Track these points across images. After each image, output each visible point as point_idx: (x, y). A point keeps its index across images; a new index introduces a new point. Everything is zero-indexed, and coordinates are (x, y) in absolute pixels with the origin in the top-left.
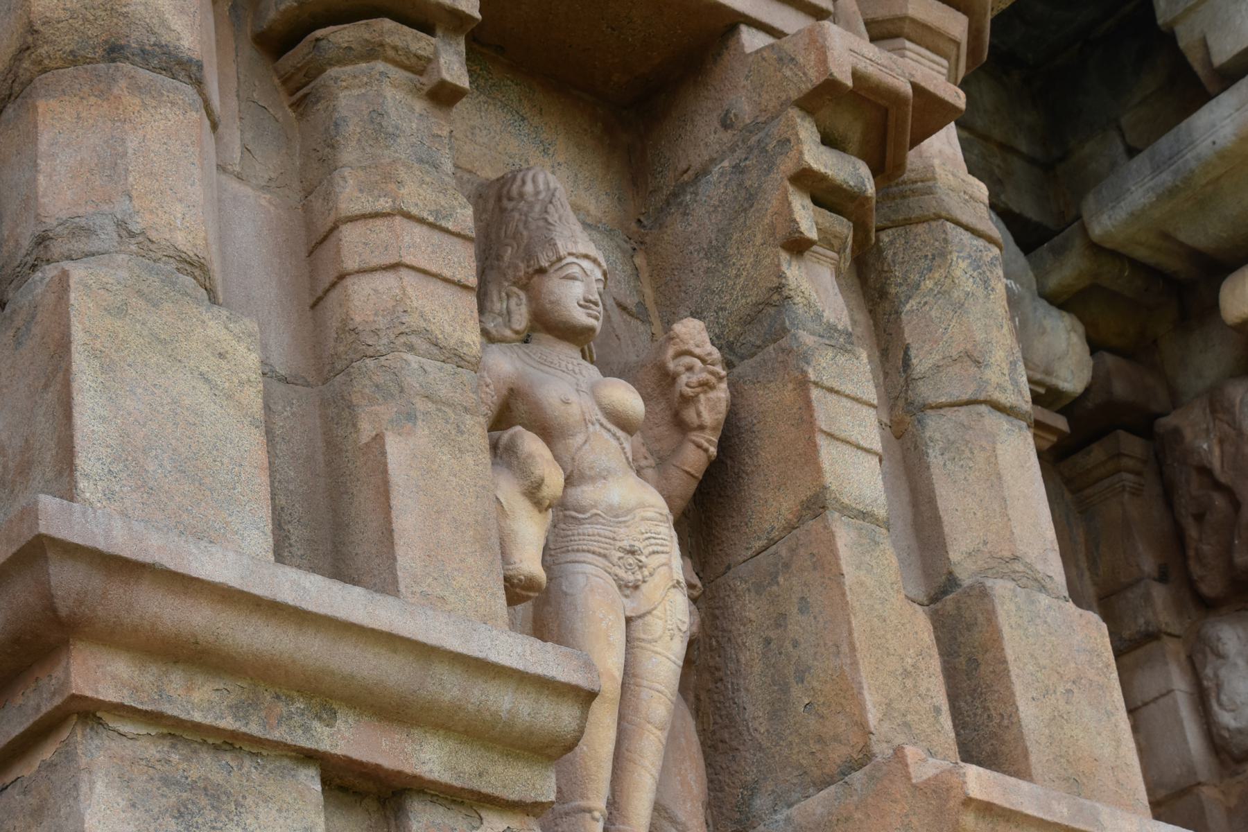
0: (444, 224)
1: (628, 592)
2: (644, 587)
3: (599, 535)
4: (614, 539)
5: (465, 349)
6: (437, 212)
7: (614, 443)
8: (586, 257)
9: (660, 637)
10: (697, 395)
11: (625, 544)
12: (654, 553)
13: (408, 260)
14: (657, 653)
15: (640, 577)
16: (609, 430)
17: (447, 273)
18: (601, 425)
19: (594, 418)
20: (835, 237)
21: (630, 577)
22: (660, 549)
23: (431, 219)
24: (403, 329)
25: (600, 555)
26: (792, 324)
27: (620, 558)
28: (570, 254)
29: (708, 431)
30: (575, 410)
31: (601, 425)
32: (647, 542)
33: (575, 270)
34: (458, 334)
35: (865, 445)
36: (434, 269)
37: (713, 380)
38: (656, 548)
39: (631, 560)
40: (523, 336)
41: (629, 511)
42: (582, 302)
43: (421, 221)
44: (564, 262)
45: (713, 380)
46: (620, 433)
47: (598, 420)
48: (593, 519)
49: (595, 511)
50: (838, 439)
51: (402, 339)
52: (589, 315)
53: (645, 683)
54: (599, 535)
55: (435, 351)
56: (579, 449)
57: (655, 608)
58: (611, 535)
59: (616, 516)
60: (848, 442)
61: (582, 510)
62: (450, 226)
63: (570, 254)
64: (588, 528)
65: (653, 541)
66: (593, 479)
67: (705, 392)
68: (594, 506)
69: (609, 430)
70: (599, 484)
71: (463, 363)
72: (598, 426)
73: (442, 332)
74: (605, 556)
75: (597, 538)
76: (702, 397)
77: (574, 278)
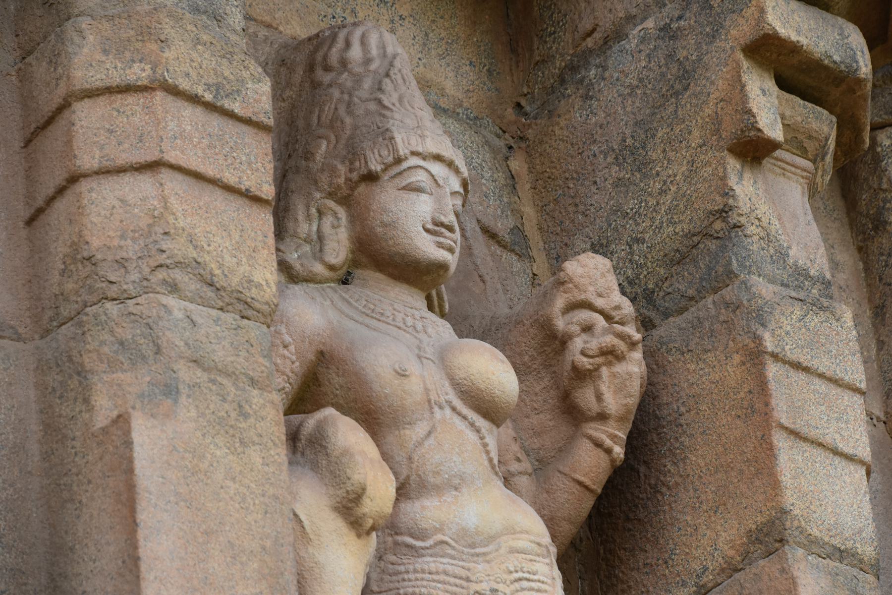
0: (227, 104)
3: (446, 573)
4: (468, 580)
5: (254, 292)
6: (218, 87)
7: (472, 436)
8: (438, 158)
10: (597, 369)
13: (172, 156)
16: (465, 418)
17: (230, 178)
18: (454, 409)
19: (442, 399)
20: (810, 137)
23: (208, 97)
24: (162, 259)
26: (742, 265)
28: (414, 153)
29: (612, 422)
30: (414, 385)
31: (454, 409)
32: (517, 585)
33: (420, 177)
34: (244, 268)
35: (848, 450)
36: (210, 171)
37: (622, 346)
40: (341, 273)
41: (492, 539)
42: (430, 226)
43: (194, 99)
44: (405, 165)
45: (622, 346)
46: (481, 422)
47: (449, 402)
48: (437, 549)
49: (439, 537)
50: (805, 439)
51: (161, 274)
52: (440, 245)
54: (446, 573)
55: (209, 293)
56: (420, 444)
58: (464, 573)
59: (472, 546)
60: (820, 445)
61: (421, 535)
62: (237, 107)
63: (414, 153)
64: (429, 563)
65: (525, 584)
66: (438, 489)
67: (609, 364)
68: (440, 530)
69: (465, 418)
70: (448, 497)
71: (250, 313)
72: (448, 411)
73: (221, 266)
75: (442, 577)
76: (604, 371)
77: (419, 190)
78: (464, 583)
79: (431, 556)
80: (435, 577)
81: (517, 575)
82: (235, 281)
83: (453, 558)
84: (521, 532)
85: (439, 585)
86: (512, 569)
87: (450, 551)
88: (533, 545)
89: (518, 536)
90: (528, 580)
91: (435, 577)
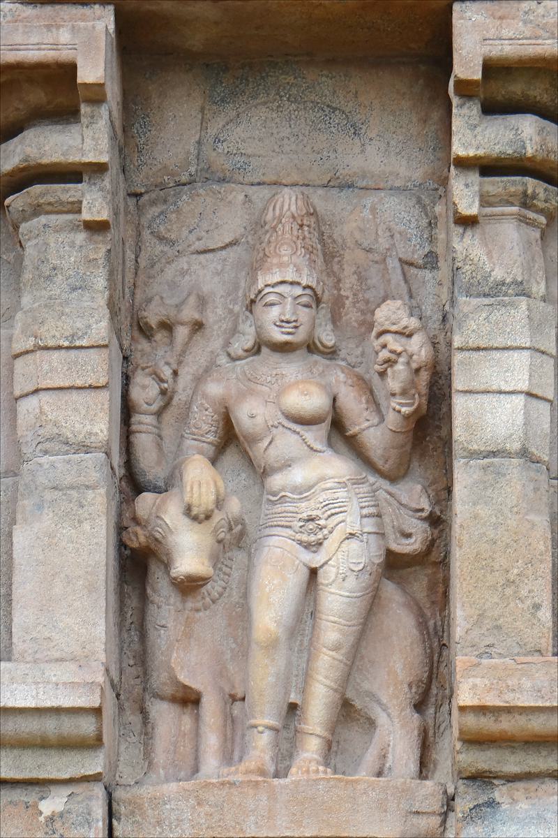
1: (314, 549)
2: (326, 543)
7: (296, 437)
8: (282, 282)
9: (333, 581)
10: (386, 370)
11: (304, 515)
12: (333, 515)
14: (333, 593)
15: (320, 536)
21: (312, 538)
22: (337, 510)
24: (39, 439)
25: (287, 527)
27: (301, 527)
29: (398, 397)
32: (326, 508)
37: (393, 357)
38: (333, 511)
39: (311, 525)
45: (393, 357)
46: (298, 428)
49: (283, 494)
52: (283, 333)
53: (324, 617)
57: (330, 559)
59: (301, 493)
67: (391, 366)
68: (283, 490)
72: (280, 428)
73: (72, 432)
74: (290, 527)
75: (283, 515)
78: (294, 515)
79: (280, 504)
80: (281, 515)
81: (324, 503)
82: (81, 437)
83: (290, 502)
84: (329, 479)
85: (283, 519)
86: (322, 501)
87: (290, 500)
88: (335, 484)
89: (327, 481)
90: (333, 504)
91: (281, 515)
